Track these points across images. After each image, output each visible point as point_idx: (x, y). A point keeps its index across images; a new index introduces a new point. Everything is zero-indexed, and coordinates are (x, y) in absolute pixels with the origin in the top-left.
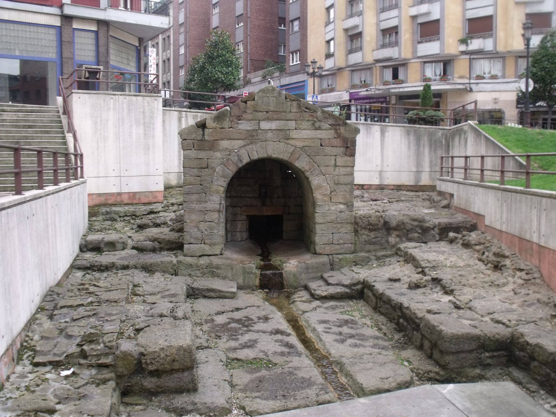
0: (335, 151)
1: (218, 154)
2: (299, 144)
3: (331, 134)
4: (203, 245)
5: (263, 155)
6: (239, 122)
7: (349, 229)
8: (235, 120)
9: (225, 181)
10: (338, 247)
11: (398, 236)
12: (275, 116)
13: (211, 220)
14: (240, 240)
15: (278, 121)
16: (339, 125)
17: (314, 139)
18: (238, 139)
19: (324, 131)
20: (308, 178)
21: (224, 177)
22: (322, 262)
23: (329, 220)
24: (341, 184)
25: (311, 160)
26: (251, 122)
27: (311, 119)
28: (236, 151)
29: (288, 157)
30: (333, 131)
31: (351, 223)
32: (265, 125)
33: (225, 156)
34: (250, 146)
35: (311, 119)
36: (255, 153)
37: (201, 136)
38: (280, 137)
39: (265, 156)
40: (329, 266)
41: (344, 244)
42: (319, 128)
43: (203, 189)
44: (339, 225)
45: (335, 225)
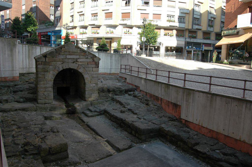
1: (51, 67)
2: (80, 63)
3: (91, 60)
4: (45, 100)
5: (67, 67)
6: (59, 55)
9: (54, 77)
11: (112, 94)
12: (72, 54)
16: (94, 57)
18: (58, 62)
20: (83, 75)
21: (53, 75)
29: (76, 68)
31: (97, 90)
33: (54, 68)
39: (68, 68)
42: (87, 58)
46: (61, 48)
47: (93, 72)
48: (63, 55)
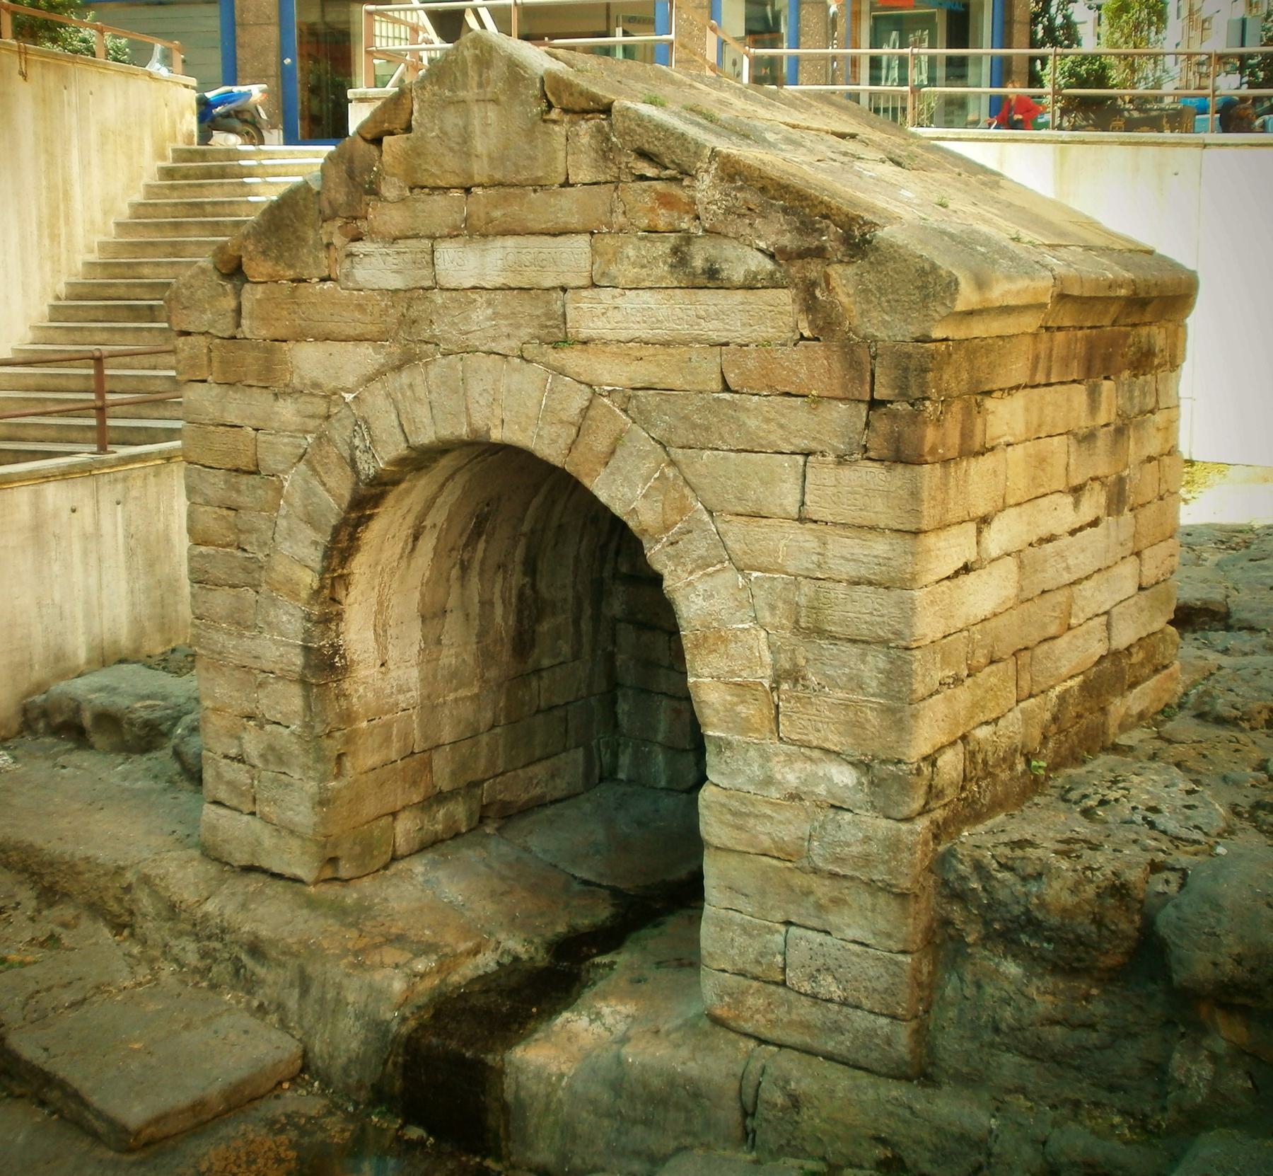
0: (800, 423)
1: (287, 411)
2: (612, 372)
4: (256, 824)
7: (882, 924)
8: (338, 240)
9: (315, 543)
10: (805, 1010)
13: (278, 717)
14: (663, 783)
15: (510, 242)
17: (685, 343)
19: (739, 295)
21: (311, 521)
22: (690, 1080)
23: (767, 843)
24: (833, 638)
25: (671, 472)
26: (401, 245)
27: (663, 218)
28: (349, 397)
30: (785, 298)
32: (461, 264)
33: (312, 424)
34: (405, 378)
35: (663, 218)
36: (422, 413)
37: (230, 318)
38: (525, 332)
40: (729, 1115)
41: (844, 1003)
43: (246, 570)
44: (823, 889)
45: (799, 880)
46: (377, 141)
47: (805, 538)
48: (395, 239)
